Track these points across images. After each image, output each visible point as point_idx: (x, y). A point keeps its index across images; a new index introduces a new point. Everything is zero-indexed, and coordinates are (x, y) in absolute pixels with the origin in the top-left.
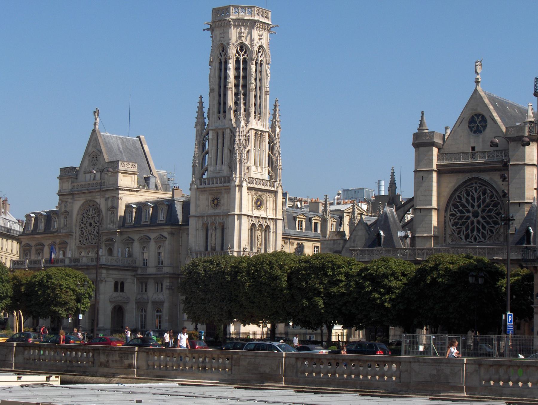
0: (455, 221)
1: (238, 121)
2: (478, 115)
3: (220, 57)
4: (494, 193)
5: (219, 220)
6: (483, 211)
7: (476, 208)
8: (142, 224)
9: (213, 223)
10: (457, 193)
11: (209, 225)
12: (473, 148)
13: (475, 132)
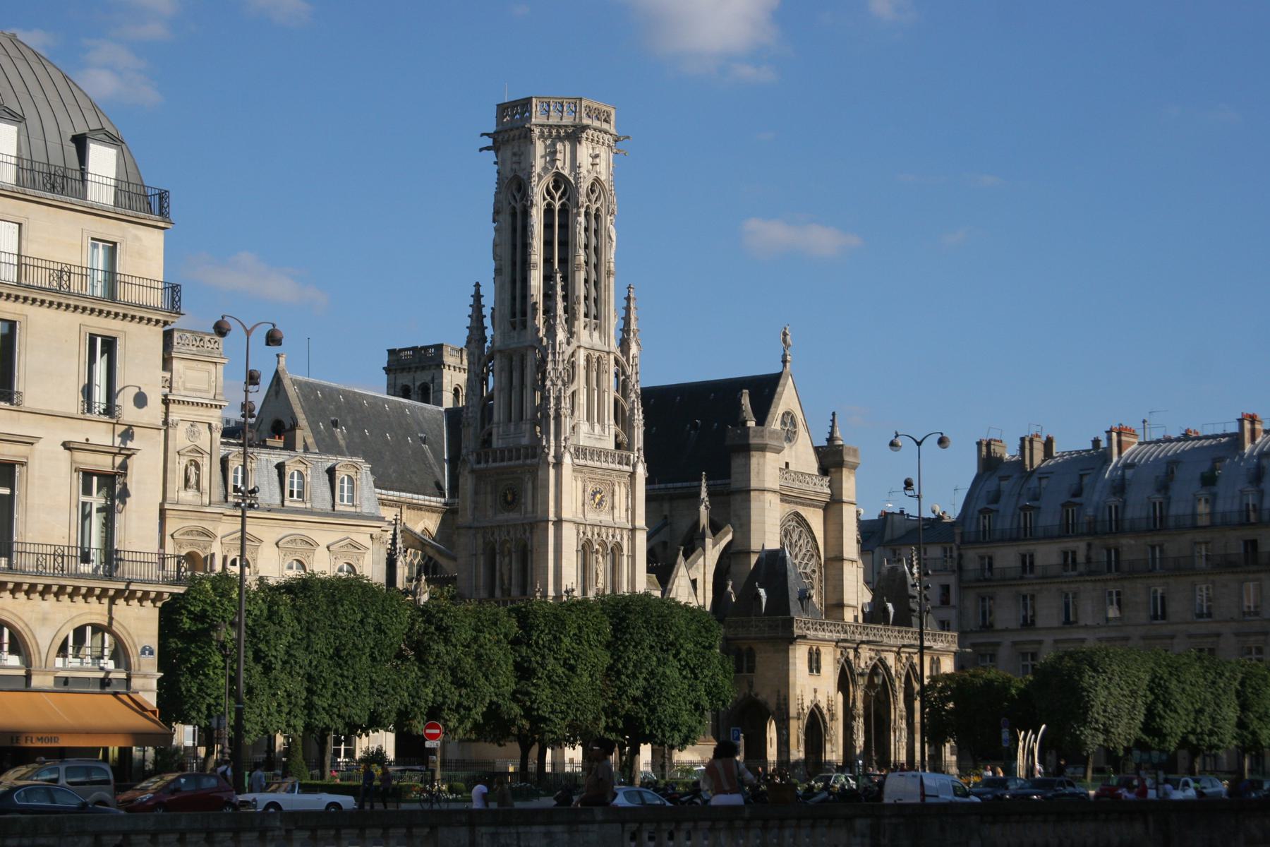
1: (551, 332)
8: (286, 503)
12: (787, 464)
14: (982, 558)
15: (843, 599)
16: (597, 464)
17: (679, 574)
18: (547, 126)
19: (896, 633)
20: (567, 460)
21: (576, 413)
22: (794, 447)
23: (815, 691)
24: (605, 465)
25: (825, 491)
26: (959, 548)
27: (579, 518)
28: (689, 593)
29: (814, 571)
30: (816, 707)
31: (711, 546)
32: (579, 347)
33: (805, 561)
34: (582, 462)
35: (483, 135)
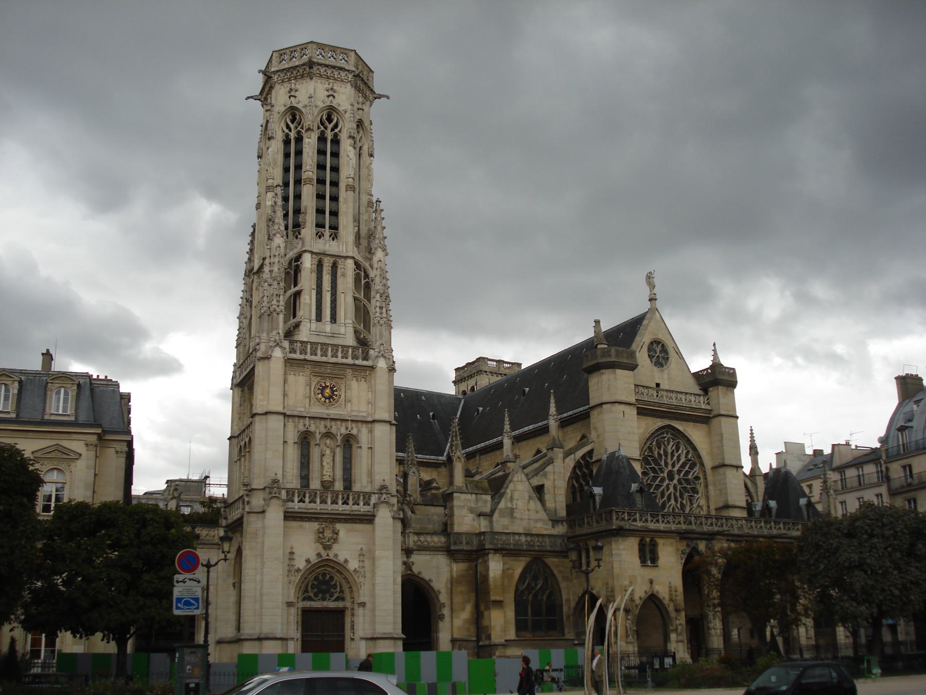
0: (649, 482)
2: (656, 342)
3: (322, 128)
4: (690, 449)
5: (340, 430)
6: (679, 472)
7: (670, 468)
9: (328, 435)
10: (649, 443)
11: (318, 436)
12: (658, 385)
13: (655, 365)
14: (904, 467)
15: (727, 500)
16: (324, 359)
17: (515, 479)
18: (283, 70)
19: (763, 524)
20: (278, 353)
21: (300, 313)
22: (666, 371)
23: (651, 582)
24: (334, 360)
25: (703, 407)
26: (885, 463)
27: (300, 410)
28: (530, 498)
29: (697, 478)
30: (652, 599)
31: (561, 455)
32: (305, 251)
33: (687, 468)
34: (297, 356)
35: (249, 98)
